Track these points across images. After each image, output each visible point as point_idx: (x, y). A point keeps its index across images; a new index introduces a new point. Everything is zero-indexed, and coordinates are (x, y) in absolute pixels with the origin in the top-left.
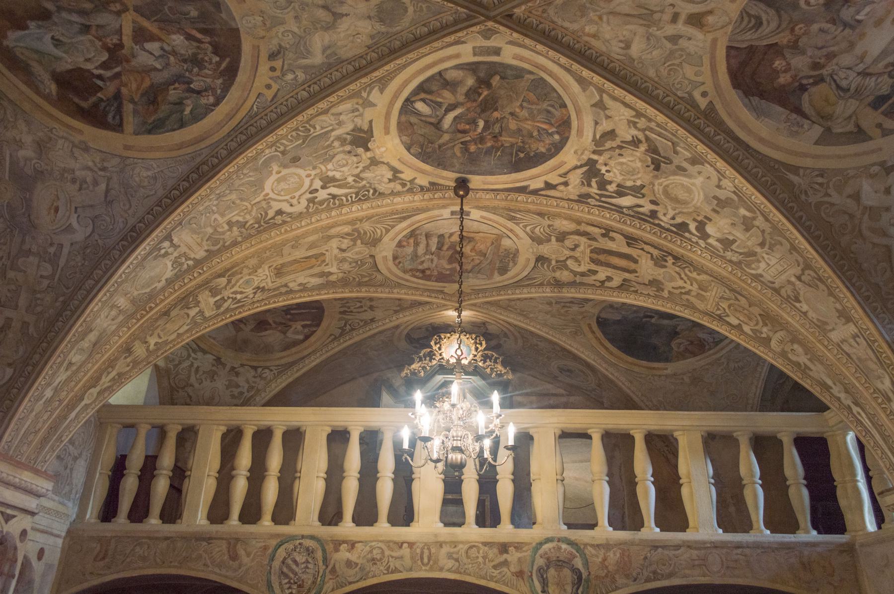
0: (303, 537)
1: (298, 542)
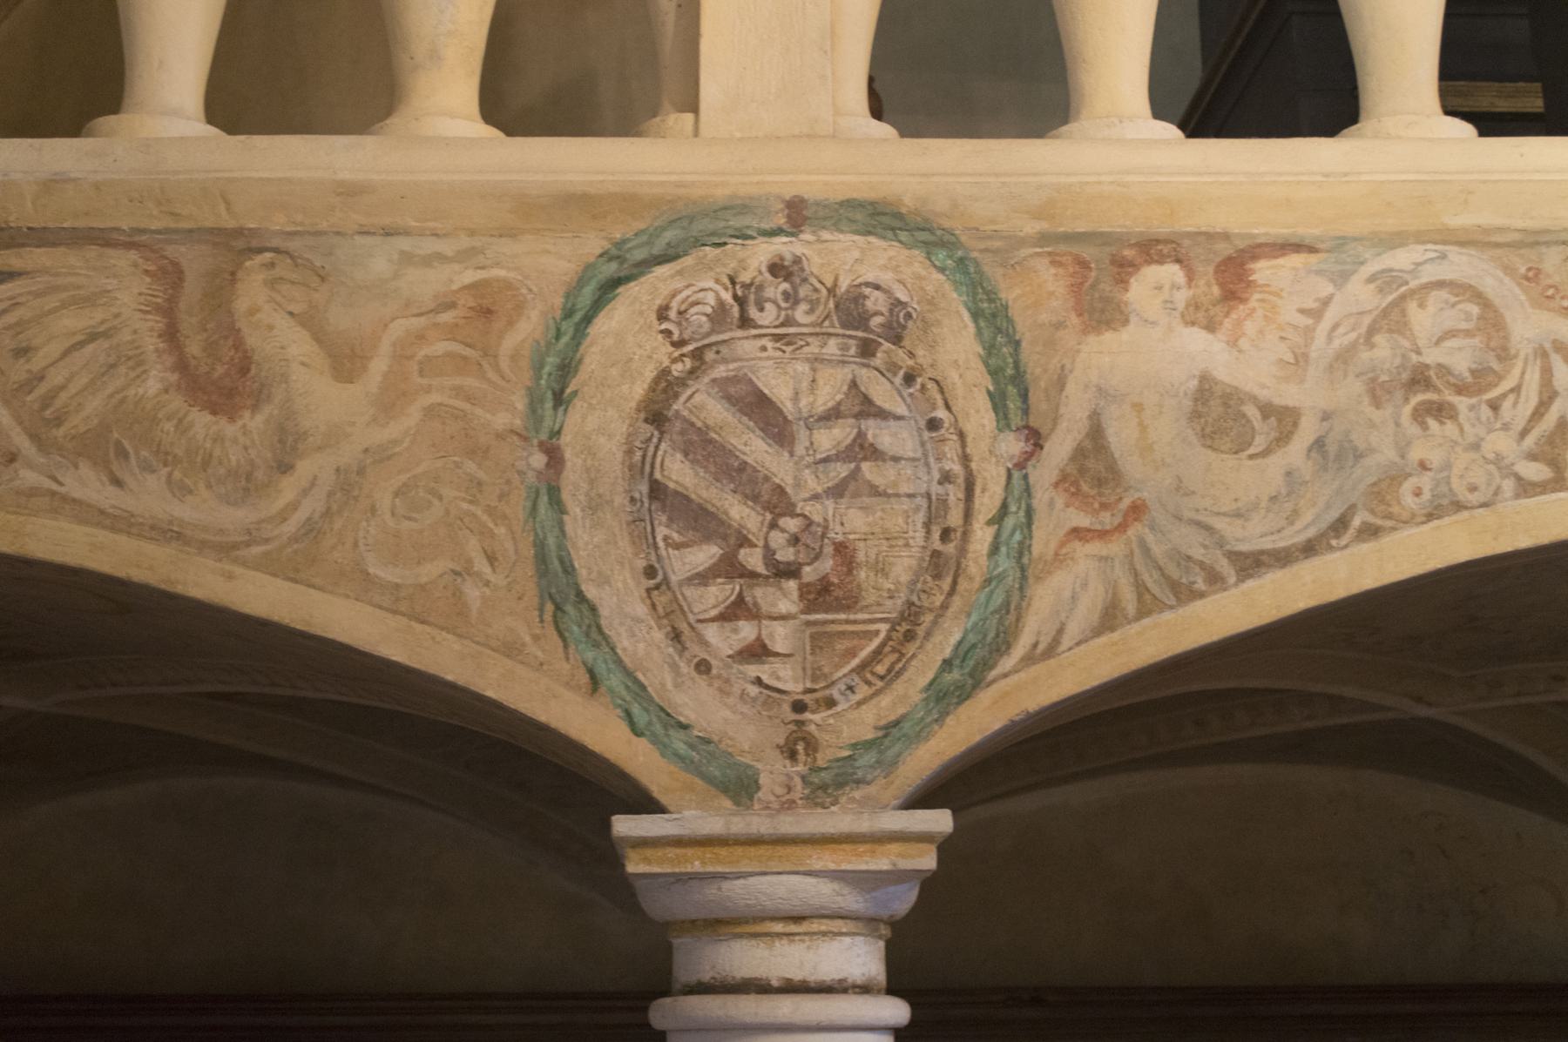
0: (798, 215)
1: (762, 253)
